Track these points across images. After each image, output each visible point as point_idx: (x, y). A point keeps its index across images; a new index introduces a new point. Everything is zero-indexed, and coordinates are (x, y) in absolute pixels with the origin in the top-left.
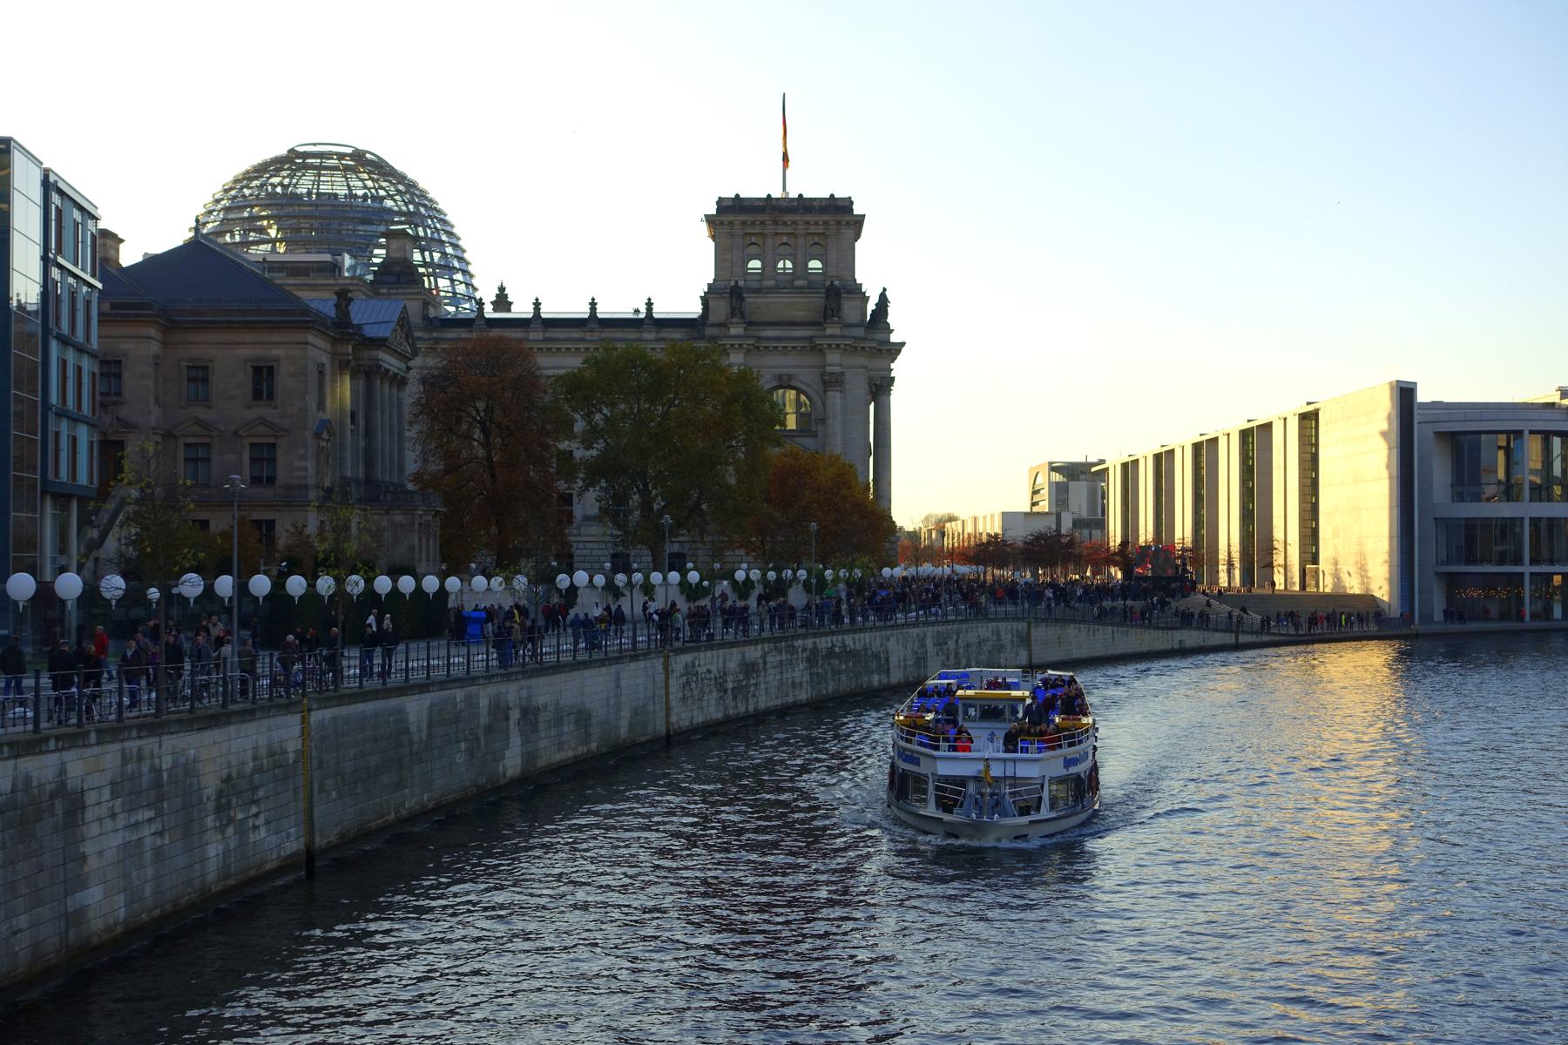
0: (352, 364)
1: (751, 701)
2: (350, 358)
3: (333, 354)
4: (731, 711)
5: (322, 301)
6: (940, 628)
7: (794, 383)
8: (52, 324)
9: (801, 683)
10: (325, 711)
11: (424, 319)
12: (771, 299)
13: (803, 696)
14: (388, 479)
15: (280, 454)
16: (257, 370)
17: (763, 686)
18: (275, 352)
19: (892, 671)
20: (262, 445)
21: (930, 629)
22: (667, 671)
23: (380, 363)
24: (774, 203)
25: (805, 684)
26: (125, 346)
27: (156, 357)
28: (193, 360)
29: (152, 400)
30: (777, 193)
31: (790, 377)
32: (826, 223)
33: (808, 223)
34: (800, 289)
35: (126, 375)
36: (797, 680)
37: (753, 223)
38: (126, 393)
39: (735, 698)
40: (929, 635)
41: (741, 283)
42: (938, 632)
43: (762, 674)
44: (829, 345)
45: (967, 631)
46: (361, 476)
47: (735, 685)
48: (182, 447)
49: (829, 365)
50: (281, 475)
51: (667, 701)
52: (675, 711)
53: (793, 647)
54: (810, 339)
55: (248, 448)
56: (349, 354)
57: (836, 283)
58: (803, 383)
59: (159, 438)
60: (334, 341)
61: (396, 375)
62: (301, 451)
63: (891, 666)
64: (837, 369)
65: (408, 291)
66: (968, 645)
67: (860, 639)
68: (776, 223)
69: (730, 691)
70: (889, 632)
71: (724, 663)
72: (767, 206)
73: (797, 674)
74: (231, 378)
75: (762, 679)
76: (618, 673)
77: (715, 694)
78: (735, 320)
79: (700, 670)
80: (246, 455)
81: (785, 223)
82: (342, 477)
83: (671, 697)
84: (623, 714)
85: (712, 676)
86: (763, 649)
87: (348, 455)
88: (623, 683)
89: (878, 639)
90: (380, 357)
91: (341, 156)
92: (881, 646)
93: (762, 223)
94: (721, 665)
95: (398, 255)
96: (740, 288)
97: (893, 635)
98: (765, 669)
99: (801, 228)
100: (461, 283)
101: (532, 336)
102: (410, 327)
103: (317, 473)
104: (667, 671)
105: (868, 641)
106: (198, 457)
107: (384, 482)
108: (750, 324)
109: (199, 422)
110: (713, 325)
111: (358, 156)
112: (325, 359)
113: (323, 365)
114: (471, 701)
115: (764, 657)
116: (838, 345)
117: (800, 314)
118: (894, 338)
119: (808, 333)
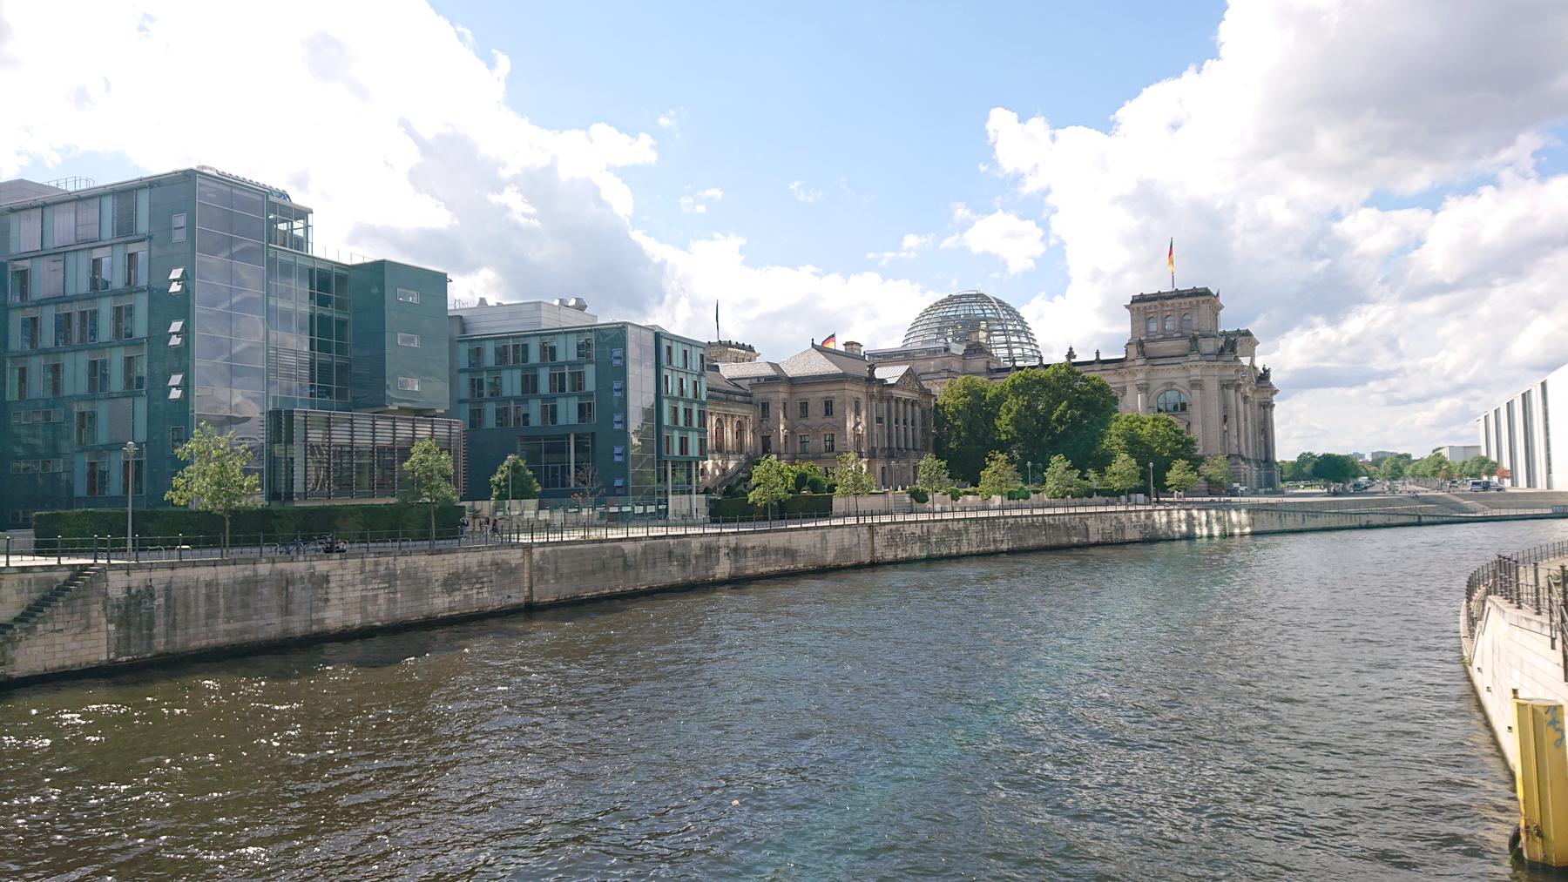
7: (1175, 387)
12: (1161, 344)
13: (1004, 547)
18: (833, 394)
31: (1172, 384)
34: (1177, 339)
51: (873, 546)
72: (1159, 297)
74: (816, 409)
89: (1077, 520)
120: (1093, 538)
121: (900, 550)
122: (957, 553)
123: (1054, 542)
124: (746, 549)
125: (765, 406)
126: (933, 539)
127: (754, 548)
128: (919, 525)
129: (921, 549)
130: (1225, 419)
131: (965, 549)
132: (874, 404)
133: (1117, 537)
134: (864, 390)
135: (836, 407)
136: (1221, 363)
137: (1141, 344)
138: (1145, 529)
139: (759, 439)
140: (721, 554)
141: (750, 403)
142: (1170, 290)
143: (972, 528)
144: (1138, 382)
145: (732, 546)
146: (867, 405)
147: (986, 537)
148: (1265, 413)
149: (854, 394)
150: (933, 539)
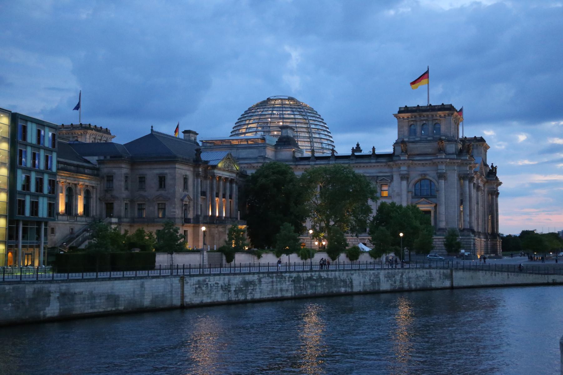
12: (418, 145)
15: (167, 206)
17: (258, 290)
24: (420, 108)
26: (114, 170)
29: (123, 189)
31: (425, 175)
34: (429, 141)
35: (114, 180)
44: (439, 162)
49: (439, 170)
53: (282, 276)
62: (174, 206)
75: (257, 287)
80: (156, 207)
85: (220, 285)
117: (430, 151)
125: (110, 178)
126: (233, 289)
130: (462, 202)
131: (257, 296)
132: (199, 180)
134: (192, 169)
135: (169, 181)
136: (459, 161)
139: (104, 206)
141: (97, 175)
142: (426, 105)
144: (402, 172)
146: (194, 181)
148: (492, 198)
149: (183, 172)
150: (233, 289)
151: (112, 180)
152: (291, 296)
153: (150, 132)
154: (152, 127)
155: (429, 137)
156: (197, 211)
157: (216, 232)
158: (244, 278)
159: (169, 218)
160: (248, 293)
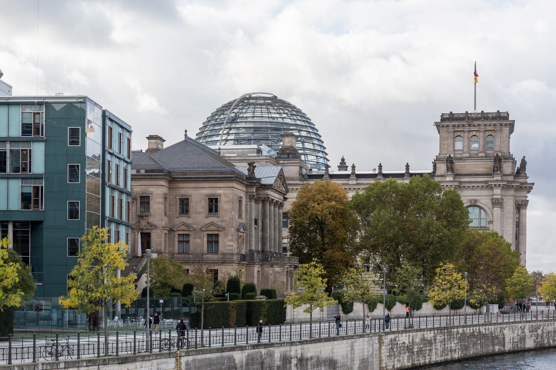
0: (255, 197)
1: (427, 357)
2: (255, 194)
3: (247, 192)
4: (416, 362)
5: (243, 168)
6: (533, 324)
7: (478, 204)
8: (106, 180)
9: (455, 350)
10: (189, 357)
11: (300, 175)
13: (456, 356)
14: (277, 251)
15: (220, 238)
16: (211, 200)
17: (434, 351)
19: (506, 344)
20: (212, 235)
21: (528, 324)
22: (381, 342)
23: (269, 196)
25: (457, 350)
26: (151, 189)
27: (165, 194)
28: (182, 195)
29: (163, 214)
30: (471, 111)
32: (495, 125)
33: (485, 125)
35: (151, 203)
36: (453, 348)
37: (459, 126)
38: (152, 210)
39: (418, 356)
40: (527, 327)
41: (452, 155)
42: (532, 326)
43: (434, 345)
44: (495, 185)
45: (548, 325)
46: (260, 249)
47: (419, 349)
48: (177, 236)
50: (221, 248)
51: (380, 357)
52: (384, 361)
54: (486, 182)
55: (206, 236)
56: (254, 192)
57: (500, 154)
58: (482, 204)
59: (167, 232)
60: (247, 186)
61: (277, 202)
63: (506, 341)
64: (499, 197)
65: (293, 162)
66: (549, 332)
67: (488, 329)
68: (470, 125)
69: (415, 353)
70: (505, 326)
71: (413, 340)
72: (466, 118)
73: (453, 345)
76: (352, 343)
77: (407, 354)
78: (449, 173)
79: (399, 342)
80: (205, 239)
81: (474, 126)
82: (250, 250)
83: (383, 355)
84: (355, 362)
86: (434, 333)
87: (253, 239)
88: (355, 348)
89: (499, 329)
90: (269, 193)
91: (265, 98)
92: (500, 332)
93: (463, 126)
94: (411, 340)
95: (288, 145)
96: (452, 158)
97: (507, 327)
98: (435, 342)
99: (482, 128)
100: (321, 157)
101: (351, 182)
102: (284, 179)
103: (238, 248)
104: (381, 342)
105: (493, 330)
106: (184, 240)
107: (270, 252)
108: (456, 175)
109: (184, 224)
110: (438, 176)
111: (274, 99)
112: (243, 195)
113: (241, 197)
114: (271, 355)
115: (435, 337)
116: (499, 185)
117: (481, 170)
118: (529, 181)
119: (485, 179)
120: (508, 347)
121: (396, 360)
122: (429, 362)
123: (485, 351)
124: (308, 359)
127: (311, 358)
128: (407, 334)
129: (408, 361)
133: (520, 346)
137: (450, 162)
138: (537, 338)
140: (293, 365)
143: (438, 338)
145: (299, 356)
146: (246, 205)
147: (446, 346)
151: (148, 203)
152: (458, 358)
153: (183, 139)
154: (186, 131)
155: (480, 153)
156: (250, 245)
157: (271, 272)
158: (423, 335)
159: (224, 254)
160: (427, 355)
